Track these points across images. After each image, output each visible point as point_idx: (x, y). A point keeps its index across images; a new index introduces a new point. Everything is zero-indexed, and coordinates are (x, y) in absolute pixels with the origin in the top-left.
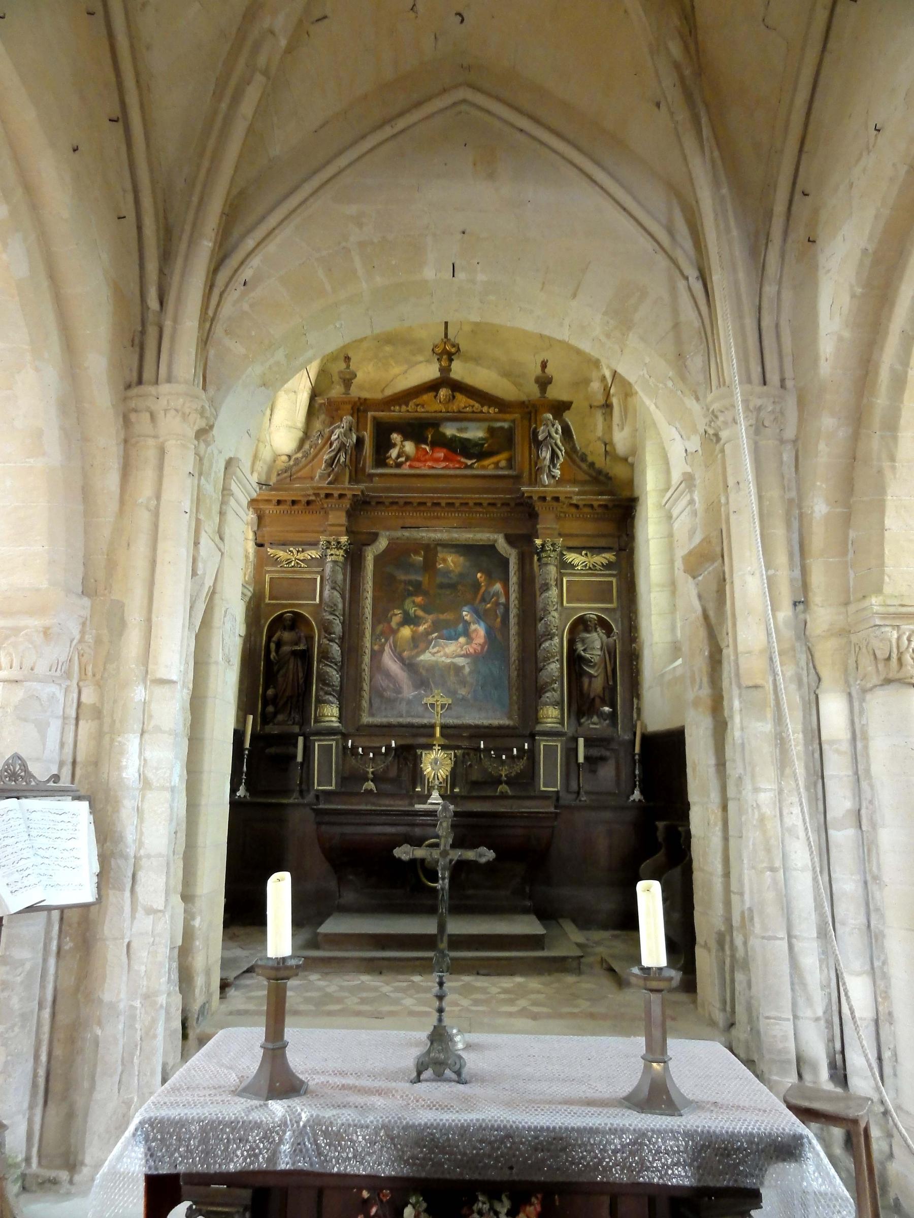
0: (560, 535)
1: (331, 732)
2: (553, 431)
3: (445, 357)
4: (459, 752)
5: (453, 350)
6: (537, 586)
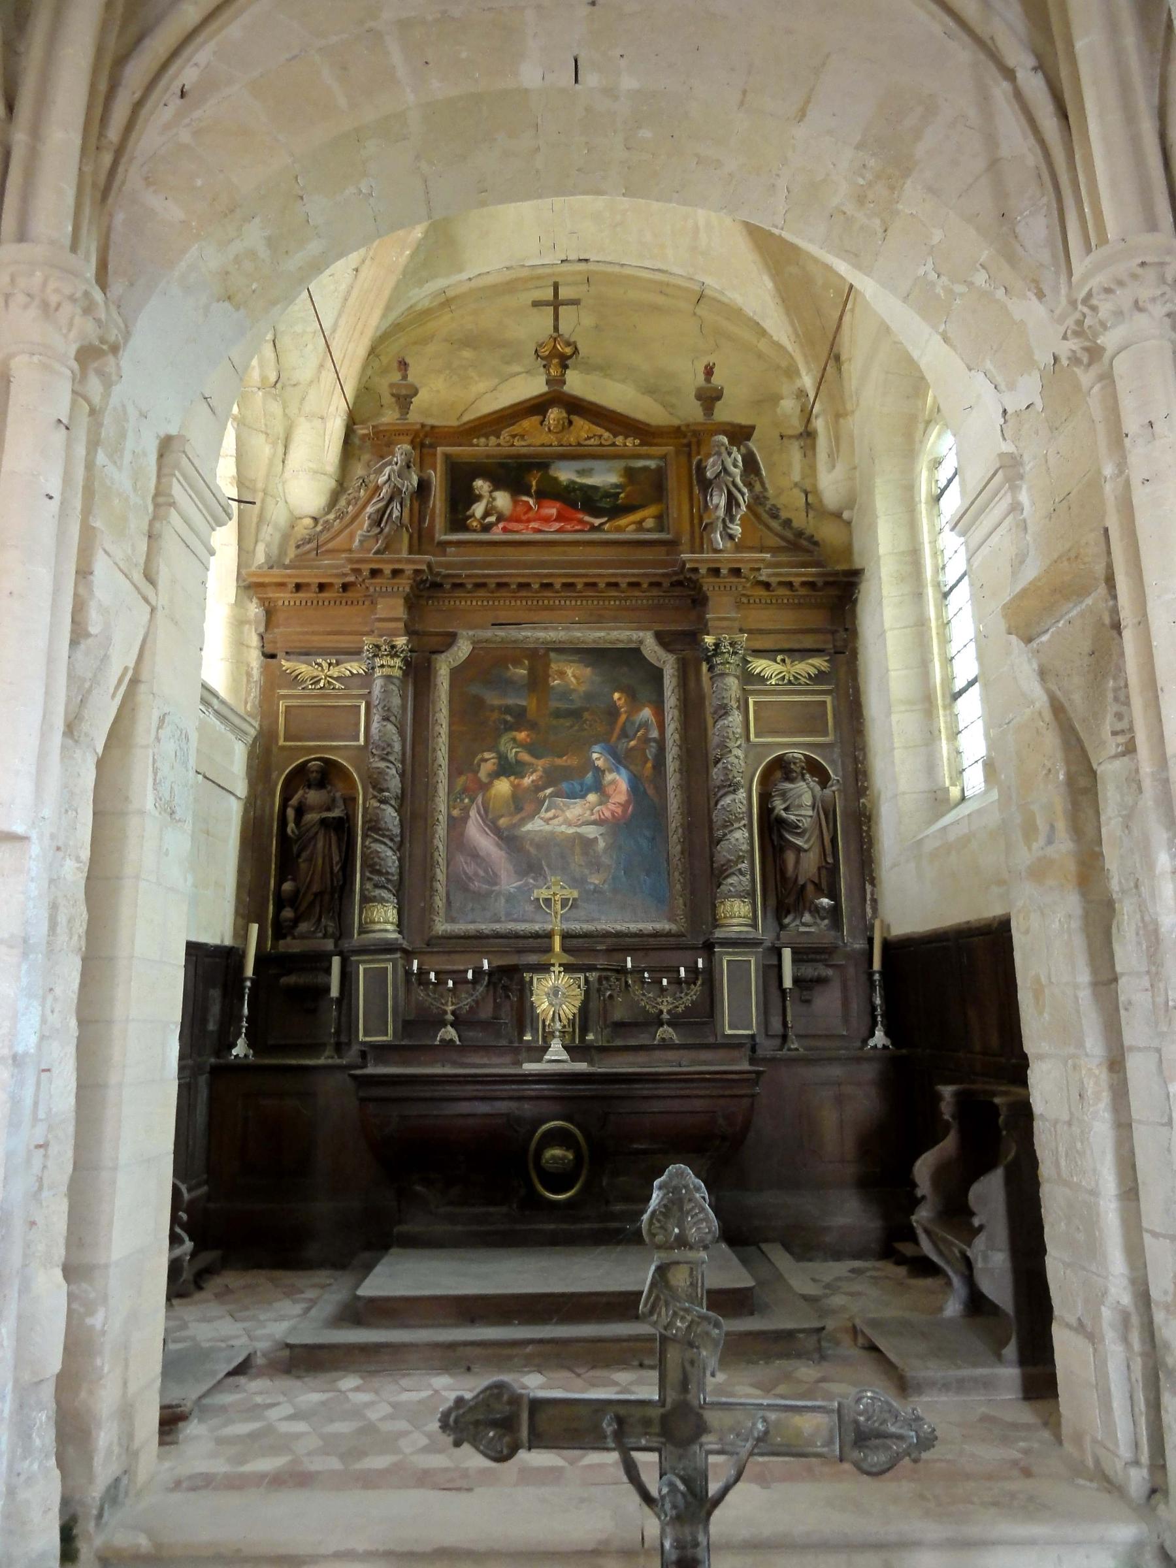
0: (741, 631)
1: (387, 948)
2: (729, 462)
3: (555, 361)
4: (593, 976)
5: (568, 351)
6: (709, 710)
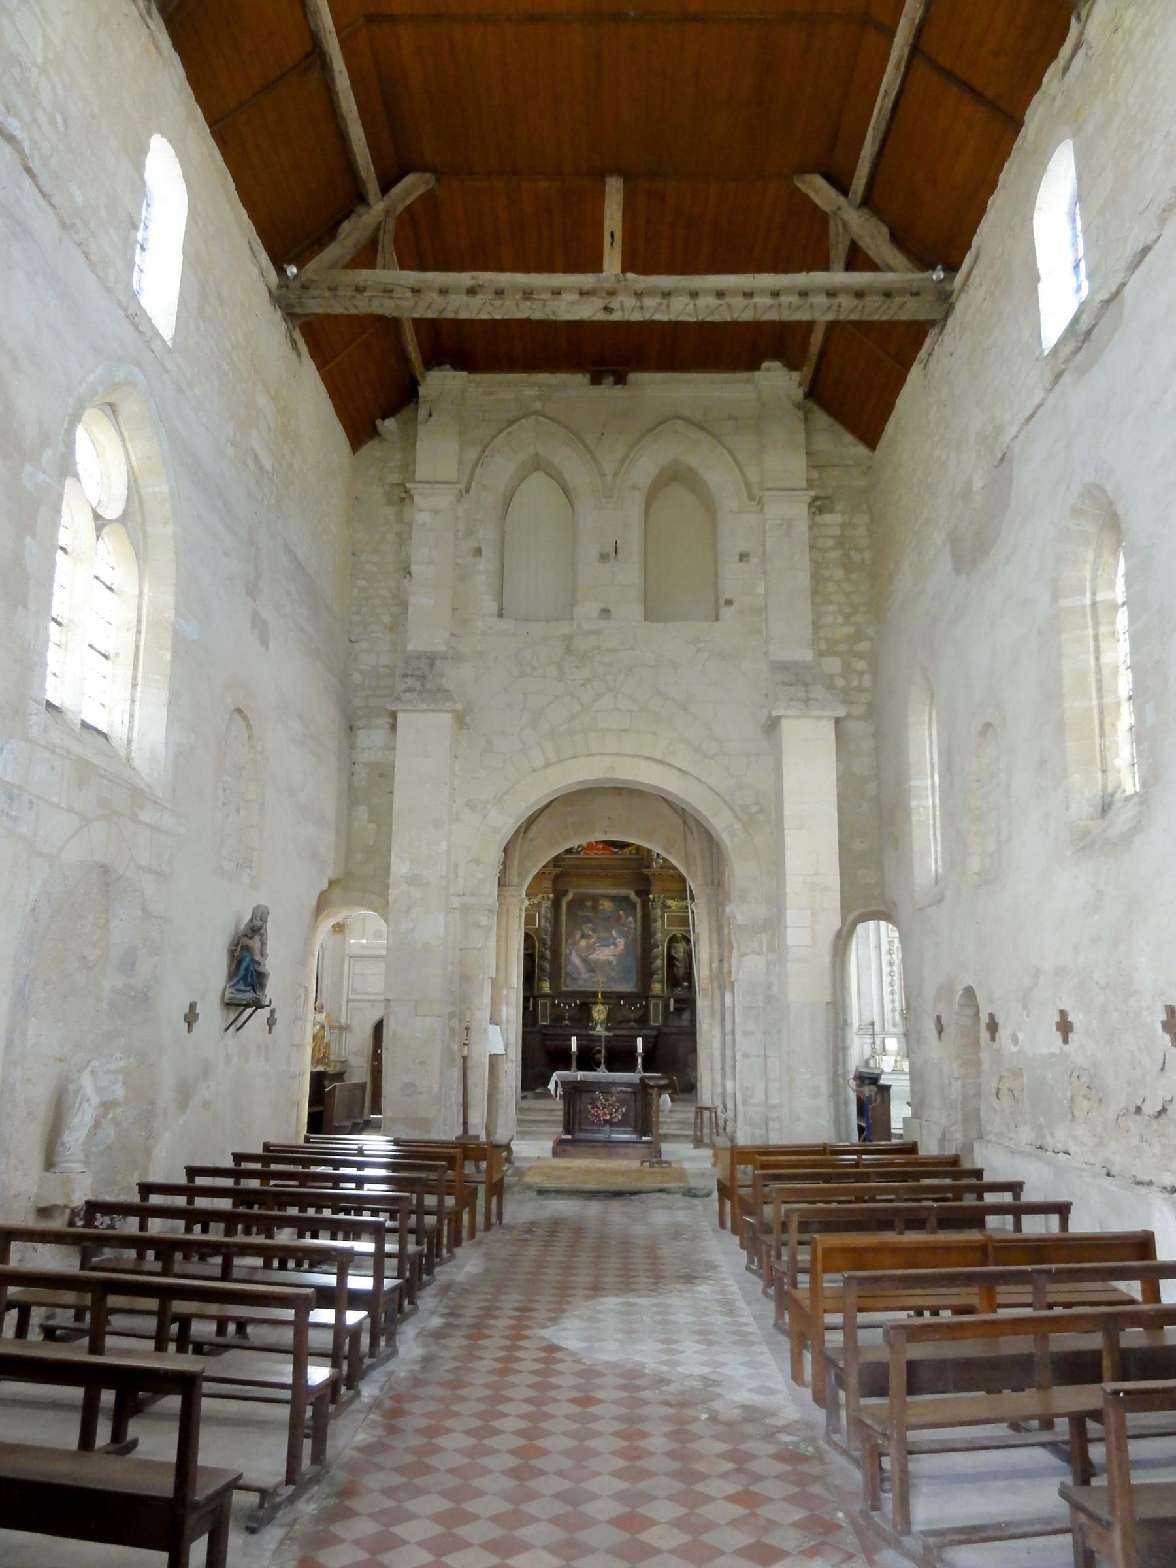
1: (546, 996)
